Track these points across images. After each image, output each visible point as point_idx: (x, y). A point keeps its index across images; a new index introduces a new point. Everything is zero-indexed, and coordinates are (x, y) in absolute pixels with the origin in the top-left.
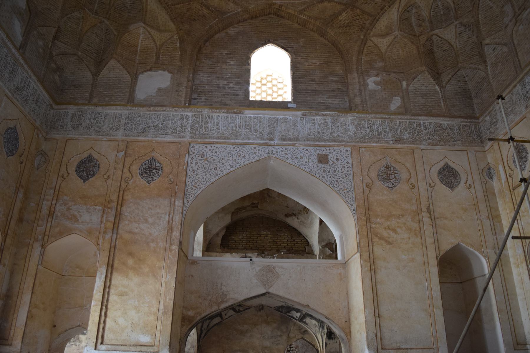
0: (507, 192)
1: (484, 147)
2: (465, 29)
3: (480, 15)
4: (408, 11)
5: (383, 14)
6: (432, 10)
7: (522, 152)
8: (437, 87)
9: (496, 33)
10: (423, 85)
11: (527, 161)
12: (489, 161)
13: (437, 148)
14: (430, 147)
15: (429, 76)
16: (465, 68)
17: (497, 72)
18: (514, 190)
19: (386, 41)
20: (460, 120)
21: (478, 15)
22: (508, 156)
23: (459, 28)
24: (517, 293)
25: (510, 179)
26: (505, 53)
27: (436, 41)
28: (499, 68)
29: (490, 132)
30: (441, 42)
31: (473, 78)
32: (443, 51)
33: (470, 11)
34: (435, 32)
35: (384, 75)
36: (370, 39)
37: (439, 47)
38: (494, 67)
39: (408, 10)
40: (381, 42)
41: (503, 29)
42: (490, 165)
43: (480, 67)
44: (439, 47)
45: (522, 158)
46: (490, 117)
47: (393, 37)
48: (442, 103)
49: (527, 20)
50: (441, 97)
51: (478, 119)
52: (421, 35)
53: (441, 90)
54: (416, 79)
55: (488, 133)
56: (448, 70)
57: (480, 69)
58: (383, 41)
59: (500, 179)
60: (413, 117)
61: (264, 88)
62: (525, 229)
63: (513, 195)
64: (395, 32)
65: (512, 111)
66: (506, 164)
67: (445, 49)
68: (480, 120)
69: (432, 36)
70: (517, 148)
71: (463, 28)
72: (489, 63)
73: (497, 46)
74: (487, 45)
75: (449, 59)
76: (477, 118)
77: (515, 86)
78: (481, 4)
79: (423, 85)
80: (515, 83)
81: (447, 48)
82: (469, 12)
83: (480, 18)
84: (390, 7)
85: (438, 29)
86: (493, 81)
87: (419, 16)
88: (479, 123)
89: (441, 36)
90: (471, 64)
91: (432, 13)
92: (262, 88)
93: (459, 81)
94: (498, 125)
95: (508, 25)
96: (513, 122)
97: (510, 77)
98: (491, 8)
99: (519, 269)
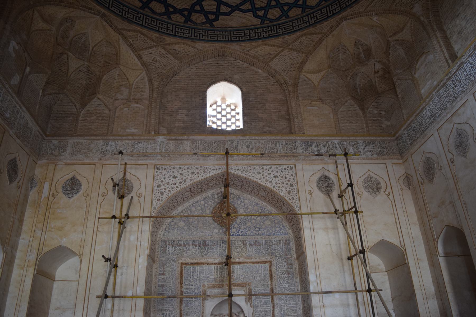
0: (43, 206)
1: (38, 160)
2: (86, 72)
3: (105, 76)
4: (66, 21)
5: (57, 5)
6: (76, 37)
7: (76, 185)
8: (41, 92)
9: (108, 97)
10: (37, 82)
11: (77, 194)
12: (36, 173)
13: (18, 140)
14: (15, 137)
15: (45, 80)
16: (67, 96)
17: (89, 119)
18: (99, 218)
19: (41, 25)
20: (39, 129)
21: (105, 75)
22: (59, 180)
23: (84, 67)
24: (9, 290)
25: (51, 198)
26: (105, 114)
27: (63, 59)
28: (92, 118)
29: (52, 153)
30: (65, 63)
31: (64, 105)
32: (59, 69)
33: (100, 66)
34: (70, 54)
35: (21, 48)
36: (34, 10)
37: (60, 64)
38: (88, 113)
39: (68, 20)
40: (38, 21)
41: (114, 99)
42: (35, 176)
43: (77, 104)
44: (60, 64)
45: (73, 189)
46: (58, 142)
47: (49, 28)
48: (37, 106)
49: (134, 109)
50: (39, 101)
51: (46, 136)
52: (60, 45)
53: (41, 96)
54: (38, 74)
55: (49, 153)
56: (55, 86)
57: (75, 106)
58: (40, 23)
59: (40, 193)
60: (20, 103)
61: (224, 113)
62: (46, 241)
63: (48, 211)
64: (53, 26)
65: (85, 152)
66: (53, 185)
67: (62, 69)
68: (47, 138)
69: (66, 54)
70: (73, 180)
71: (85, 70)
72: (86, 108)
73: (104, 105)
74: (98, 98)
75: (60, 78)
76: (47, 136)
77: (99, 140)
78: (112, 71)
79: (37, 82)
80: (101, 138)
81: (63, 70)
82: (99, 66)
83: (104, 77)
84: (65, 6)
85: (72, 54)
86: (81, 122)
87: (67, 30)
88: (44, 139)
89: (69, 59)
90: (73, 97)
91: (75, 38)
92: (222, 112)
93: (54, 99)
94: (63, 154)
95: (118, 99)
96: (81, 160)
97: (99, 131)
98: (114, 79)
99: (22, 271)
